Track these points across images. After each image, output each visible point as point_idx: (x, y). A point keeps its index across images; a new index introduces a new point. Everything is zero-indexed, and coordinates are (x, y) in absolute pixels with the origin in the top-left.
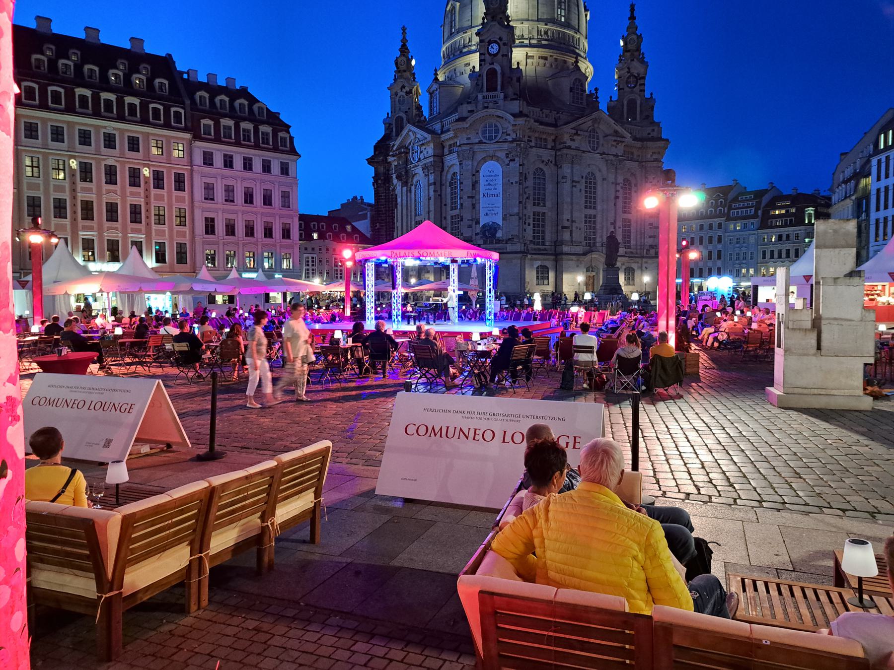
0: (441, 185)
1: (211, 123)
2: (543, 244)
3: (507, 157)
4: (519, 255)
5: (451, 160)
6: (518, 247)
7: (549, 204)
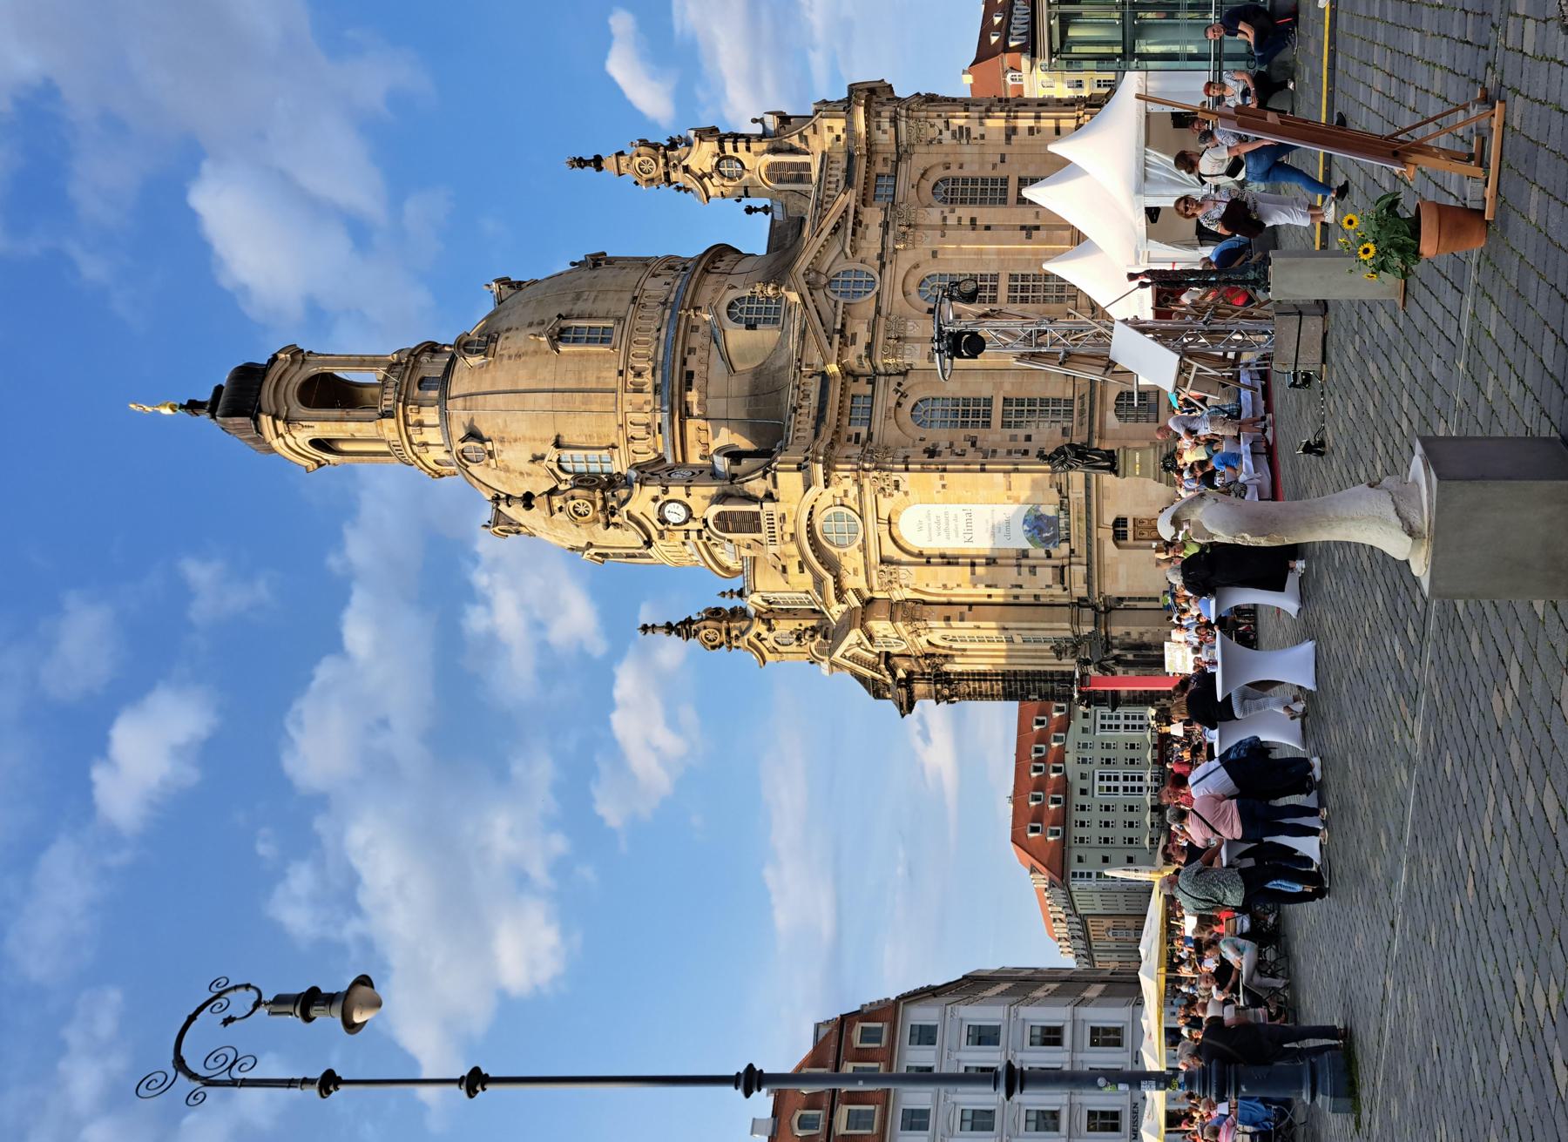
2: (1070, 402)
3: (891, 495)
5: (898, 595)
7: (986, 392)
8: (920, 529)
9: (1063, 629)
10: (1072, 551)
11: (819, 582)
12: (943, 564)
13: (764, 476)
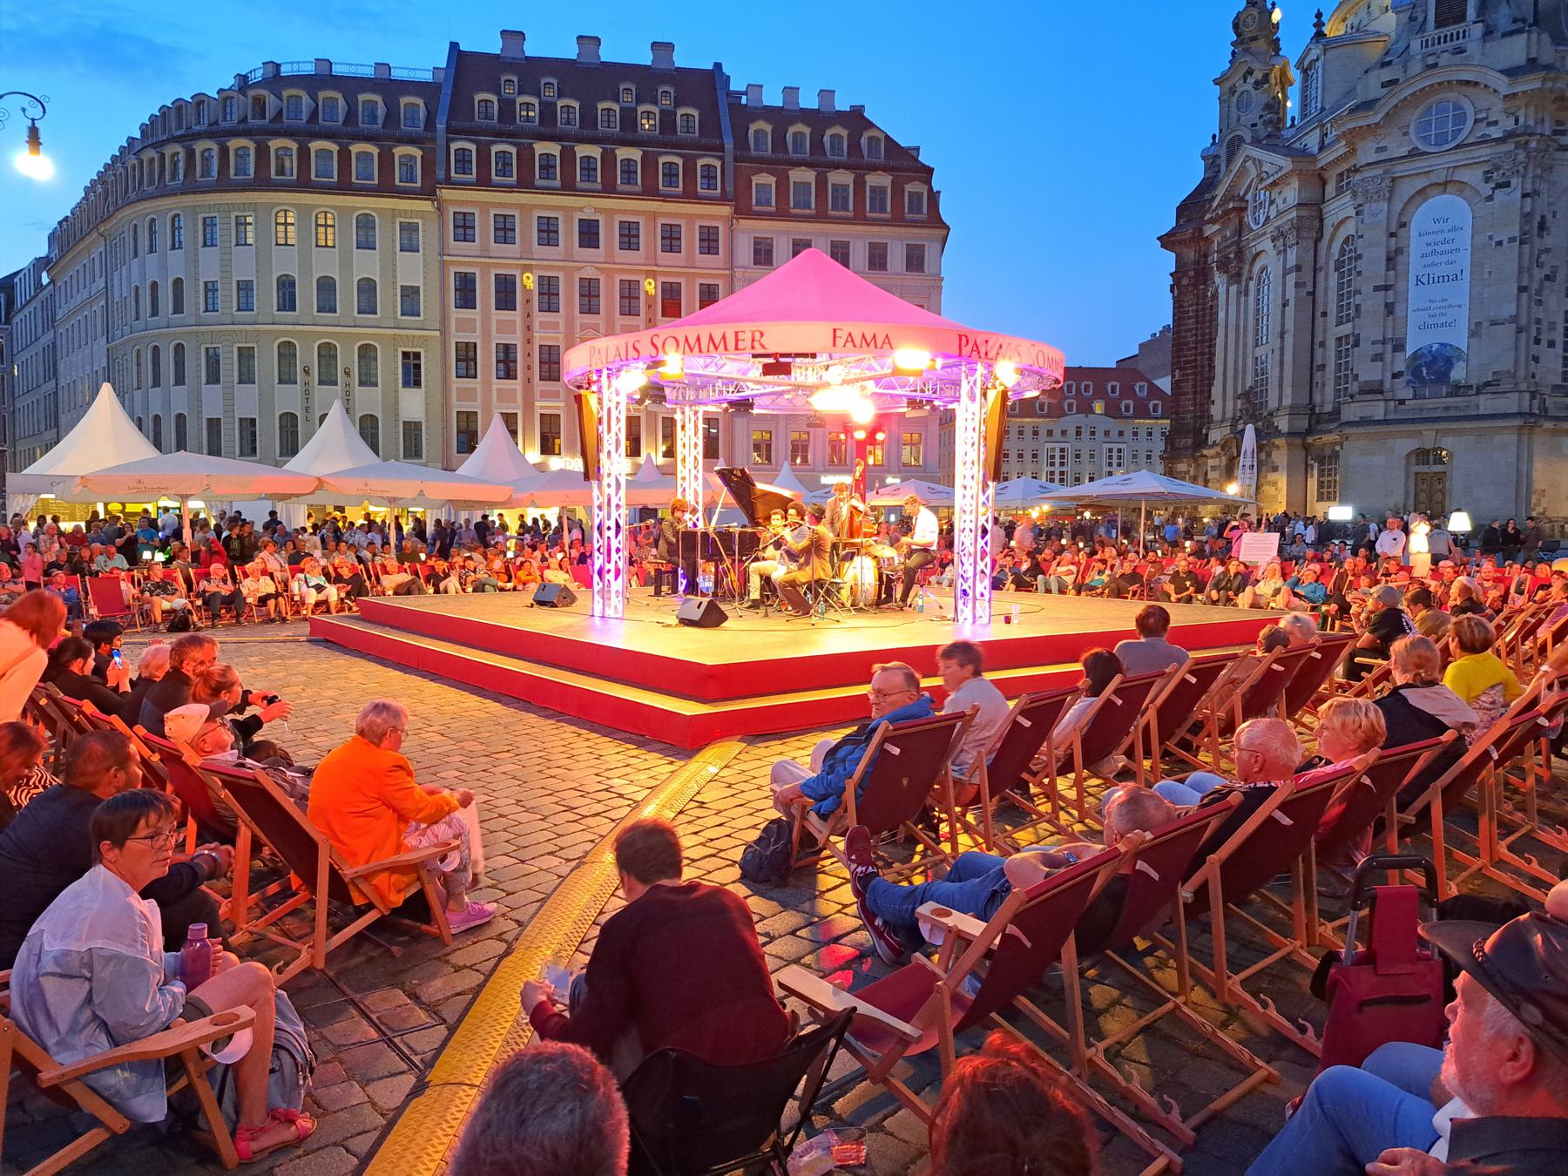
0: (1315, 270)
1: (772, 180)
3: (1487, 180)
4: (1518, 422)
5: (1339, 208)
6: (1510, 403)
8: (1437, 221)
9: (1281, 396)
10: (1402, 402)
11: (1368, 105)
12: (1388, 252)
13: (1515, 21)
